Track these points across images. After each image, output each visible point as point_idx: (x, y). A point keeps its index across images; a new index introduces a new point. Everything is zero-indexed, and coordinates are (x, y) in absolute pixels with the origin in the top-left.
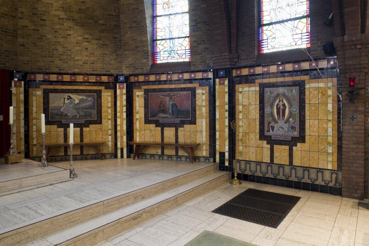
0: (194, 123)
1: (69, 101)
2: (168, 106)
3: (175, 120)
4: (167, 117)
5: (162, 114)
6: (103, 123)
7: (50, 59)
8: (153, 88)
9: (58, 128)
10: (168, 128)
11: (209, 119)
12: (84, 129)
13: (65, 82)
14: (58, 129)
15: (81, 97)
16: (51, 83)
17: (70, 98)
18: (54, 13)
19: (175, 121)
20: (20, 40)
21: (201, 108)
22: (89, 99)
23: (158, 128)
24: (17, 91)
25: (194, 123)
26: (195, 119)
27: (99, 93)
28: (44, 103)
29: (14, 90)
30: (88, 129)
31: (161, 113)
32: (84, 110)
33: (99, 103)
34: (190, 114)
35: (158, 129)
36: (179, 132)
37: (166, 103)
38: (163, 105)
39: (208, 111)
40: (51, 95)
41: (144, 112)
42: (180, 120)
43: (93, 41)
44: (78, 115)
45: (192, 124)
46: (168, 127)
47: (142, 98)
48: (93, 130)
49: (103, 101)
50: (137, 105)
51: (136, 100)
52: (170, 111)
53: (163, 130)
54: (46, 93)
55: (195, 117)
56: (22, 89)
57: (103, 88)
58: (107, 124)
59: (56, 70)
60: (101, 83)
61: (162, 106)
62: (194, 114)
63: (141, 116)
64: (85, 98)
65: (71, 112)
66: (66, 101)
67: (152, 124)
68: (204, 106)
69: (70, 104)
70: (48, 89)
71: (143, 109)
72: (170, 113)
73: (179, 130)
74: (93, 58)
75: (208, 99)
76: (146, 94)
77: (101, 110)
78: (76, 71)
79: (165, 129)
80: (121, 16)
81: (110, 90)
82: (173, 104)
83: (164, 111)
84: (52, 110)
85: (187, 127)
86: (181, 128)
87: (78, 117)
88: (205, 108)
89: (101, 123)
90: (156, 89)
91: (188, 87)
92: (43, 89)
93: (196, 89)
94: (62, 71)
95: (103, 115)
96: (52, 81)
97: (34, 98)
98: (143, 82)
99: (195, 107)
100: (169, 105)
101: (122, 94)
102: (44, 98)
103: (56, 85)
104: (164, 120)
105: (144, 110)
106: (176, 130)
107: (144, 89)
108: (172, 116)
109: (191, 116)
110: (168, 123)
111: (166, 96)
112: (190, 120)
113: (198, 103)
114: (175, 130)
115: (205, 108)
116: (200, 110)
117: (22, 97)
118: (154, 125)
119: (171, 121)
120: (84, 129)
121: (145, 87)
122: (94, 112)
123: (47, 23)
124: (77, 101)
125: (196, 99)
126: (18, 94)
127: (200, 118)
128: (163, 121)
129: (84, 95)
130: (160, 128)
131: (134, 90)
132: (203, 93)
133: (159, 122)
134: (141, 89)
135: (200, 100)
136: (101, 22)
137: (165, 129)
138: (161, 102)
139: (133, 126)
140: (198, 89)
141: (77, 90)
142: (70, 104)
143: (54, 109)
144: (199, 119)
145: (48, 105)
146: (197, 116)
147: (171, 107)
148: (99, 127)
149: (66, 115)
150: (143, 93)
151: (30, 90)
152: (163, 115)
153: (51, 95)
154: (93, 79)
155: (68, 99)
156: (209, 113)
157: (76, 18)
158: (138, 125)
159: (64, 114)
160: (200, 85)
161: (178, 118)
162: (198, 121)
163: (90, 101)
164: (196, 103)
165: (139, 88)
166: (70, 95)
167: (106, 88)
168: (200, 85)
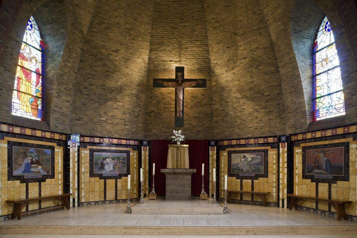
1: (244, 159)
5: (316, 170)
6: (269, 177)
7: (232, 129)
9: (236, 179)
10: (322, 184)
12: (255, 181)
13: (242, 145)
14: (237, 180)
15: (252, 156)
16: (233, 146)
17: (245, 157)
18: (233, 95)
19: (328, 177)
20: (215, 119)
22: (259, 157)
23: (313, 183)
24: (213, 153)
27: (266, 152)
28: (228, 160)
29: (211, 153)
30: (257, 181)
32: (255, 166)
33: (266, 160)
36: (332, 188)
38: (318, 161)
40: (233, 155)
41: (302, 168)
42: (333, 176)
43: (261, 111)
44: (250, 170)
48: (261, 182)
49: (269, 158)
50: (297, 162)
51: (295, 157)
52: (324, 167)
53: (318, 185)
54: (230, 154)
55: (348, 173)
56: (215, 152)
58: (272, 177)
59: (236, 137)
60: (267, 144)
64: (255, 156)
65: (246, 168)
66: (242, 159)
67: (308, 179)
69: (245, 161)
70: (230, 151)
71: (301, 165)
73: (332, 186)
74: (261, 124)
77: (268, 166)
78: (250, 135)
79: (319, 184)
80: (283, 84)
81: (275, 149)
83: (318, 167)
84: (233, 165)
85: (340, 183)
87: (250, 172)
89: (267, 177)
92: (228, 151)
94: (240, 137)
95: (269, 170)
96: (233, 145)
97: (223, 158)
98: (301, 140)
101: (283, 152)
102: (228, 157)
103: (236, 147)
105: (302, 166)
106: (329, 186)
109: (344, 172)
114: (328, 186)
117: (215, 157)
118: (310, 180)
120: (255, 181)
122: (262, 167)
123: (230, 103)
124: (250, 159)
126: (213, 156)
128: (318, 177)
129: (255, 154)
130: (315, 184)
131: (295, 148)
133: (314, 177)
136: (267, 93)
137: (319, 184)
141: (249, 150)
142: (245, 161)
143: (235, 166)
145: (231, 162)
148: (266, 180)
149: (242, 170)
151: (221, 152)
152: (318, 171)
153: (233, 155)
154: (261, 141)
155: (243, 158)
157: (248, 95)
159: (241, 169)
161: (332, 174)
163: (259, 159)
165: (298, 145)
166: (245, 154)
167: (271, 148)
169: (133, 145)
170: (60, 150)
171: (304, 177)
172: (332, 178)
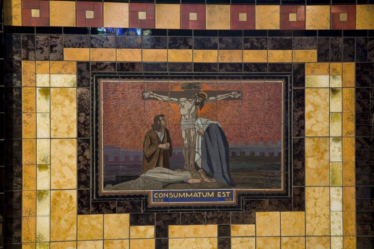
0: (298, 204)
2: (188, 135)
3: (216, 193)
4: (182, 182)
5: (161, 169)
8: (120, 59)
10: (188, 229)
11: (357, 189)
19: (215, 198)
21: (323, 146)
23: (142, 228)
25: (298, 204)
26: (302, 190)
31: (158, 165)
34: (279, 169)
35: (141, 235)
36: (233, 241)
37: (178, 126)
38: (167, 132)
39: (353, 158)
41: (79, 162)
42: (239, 195)
45: (290, 210)
46: (187, 224)
47: (67, 102)
50: (43, 132)
51: (34, 110)
52: (197, 157)
53: (166, 234)
55: (302, 181)
57: (306, 55)
61: (161, 135)
62: (296, 171)
63: (62, 181)
67: (114, 211)
68: (337, 139)
71: (72, 149)
72: (195, 164)
73: (233, 233)
75: (353, 110)
76: (84, 83)
79: (174, 230)
82: (208, 130)
83: (168, 159)
85: (268, 221)
86: (242, 225)
88: (339, 145)
90: (133, 65)
91: (271, 60)
93: (307, 70)
98: (68, 30)
99: (301, 143)
100: (192, 133)
104: (170, 193)
105: (75, 154)
106: (220, 234)
107: (79, 63)
108: (207, 180)
109: (286, 176)
110: (190, 207)
111: (178, 95)
112: (279, 194)
113: (314, 124)
114: (216, 234)
115: (339, 145)
116: (323, 153)
118: (125, 217)
119: (202, 199)
121: (84, 54)
125: (304, 110)
127: (322, 183)
128: (166, 199)
130: (151, 230)
131: (27, 67)
132: (332, 86)
133: (146, 203)
134: (61, 59)
135: (321, 116)
137: (174, 230)
138: (157, 119)
139: (19, 227)
140: (313, 72)
144: (317, 188)
146: (310, 175)
147: (199, 141)
150: (73, 78)
152: (166, 176)
156: (356, 163)
158: (47, 219)
160: (322, 57)
161: (232, 184)
162: (312, 195)
164: (303, 128)
165: (53, 53)
168: (322, 57)
169: (322, 33)
170: (42, 80)
171: (91, 201)
172: (234, 201)
